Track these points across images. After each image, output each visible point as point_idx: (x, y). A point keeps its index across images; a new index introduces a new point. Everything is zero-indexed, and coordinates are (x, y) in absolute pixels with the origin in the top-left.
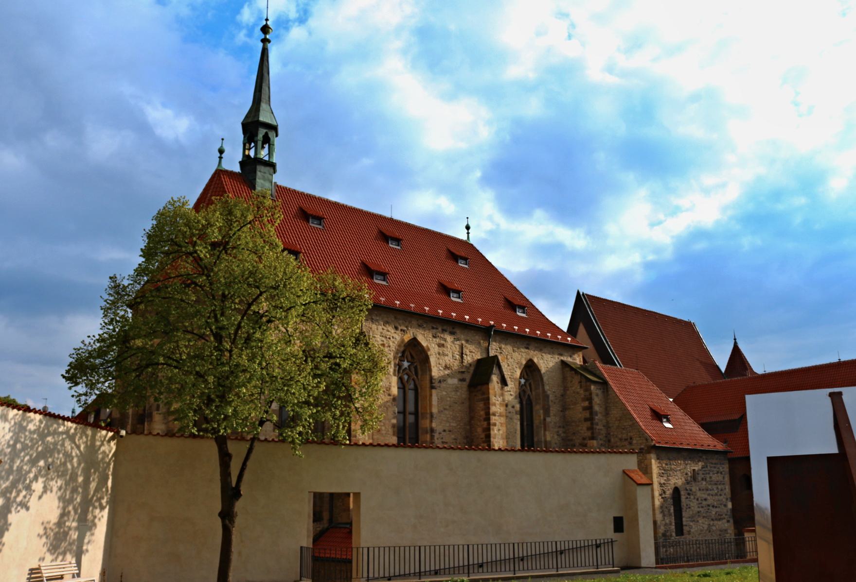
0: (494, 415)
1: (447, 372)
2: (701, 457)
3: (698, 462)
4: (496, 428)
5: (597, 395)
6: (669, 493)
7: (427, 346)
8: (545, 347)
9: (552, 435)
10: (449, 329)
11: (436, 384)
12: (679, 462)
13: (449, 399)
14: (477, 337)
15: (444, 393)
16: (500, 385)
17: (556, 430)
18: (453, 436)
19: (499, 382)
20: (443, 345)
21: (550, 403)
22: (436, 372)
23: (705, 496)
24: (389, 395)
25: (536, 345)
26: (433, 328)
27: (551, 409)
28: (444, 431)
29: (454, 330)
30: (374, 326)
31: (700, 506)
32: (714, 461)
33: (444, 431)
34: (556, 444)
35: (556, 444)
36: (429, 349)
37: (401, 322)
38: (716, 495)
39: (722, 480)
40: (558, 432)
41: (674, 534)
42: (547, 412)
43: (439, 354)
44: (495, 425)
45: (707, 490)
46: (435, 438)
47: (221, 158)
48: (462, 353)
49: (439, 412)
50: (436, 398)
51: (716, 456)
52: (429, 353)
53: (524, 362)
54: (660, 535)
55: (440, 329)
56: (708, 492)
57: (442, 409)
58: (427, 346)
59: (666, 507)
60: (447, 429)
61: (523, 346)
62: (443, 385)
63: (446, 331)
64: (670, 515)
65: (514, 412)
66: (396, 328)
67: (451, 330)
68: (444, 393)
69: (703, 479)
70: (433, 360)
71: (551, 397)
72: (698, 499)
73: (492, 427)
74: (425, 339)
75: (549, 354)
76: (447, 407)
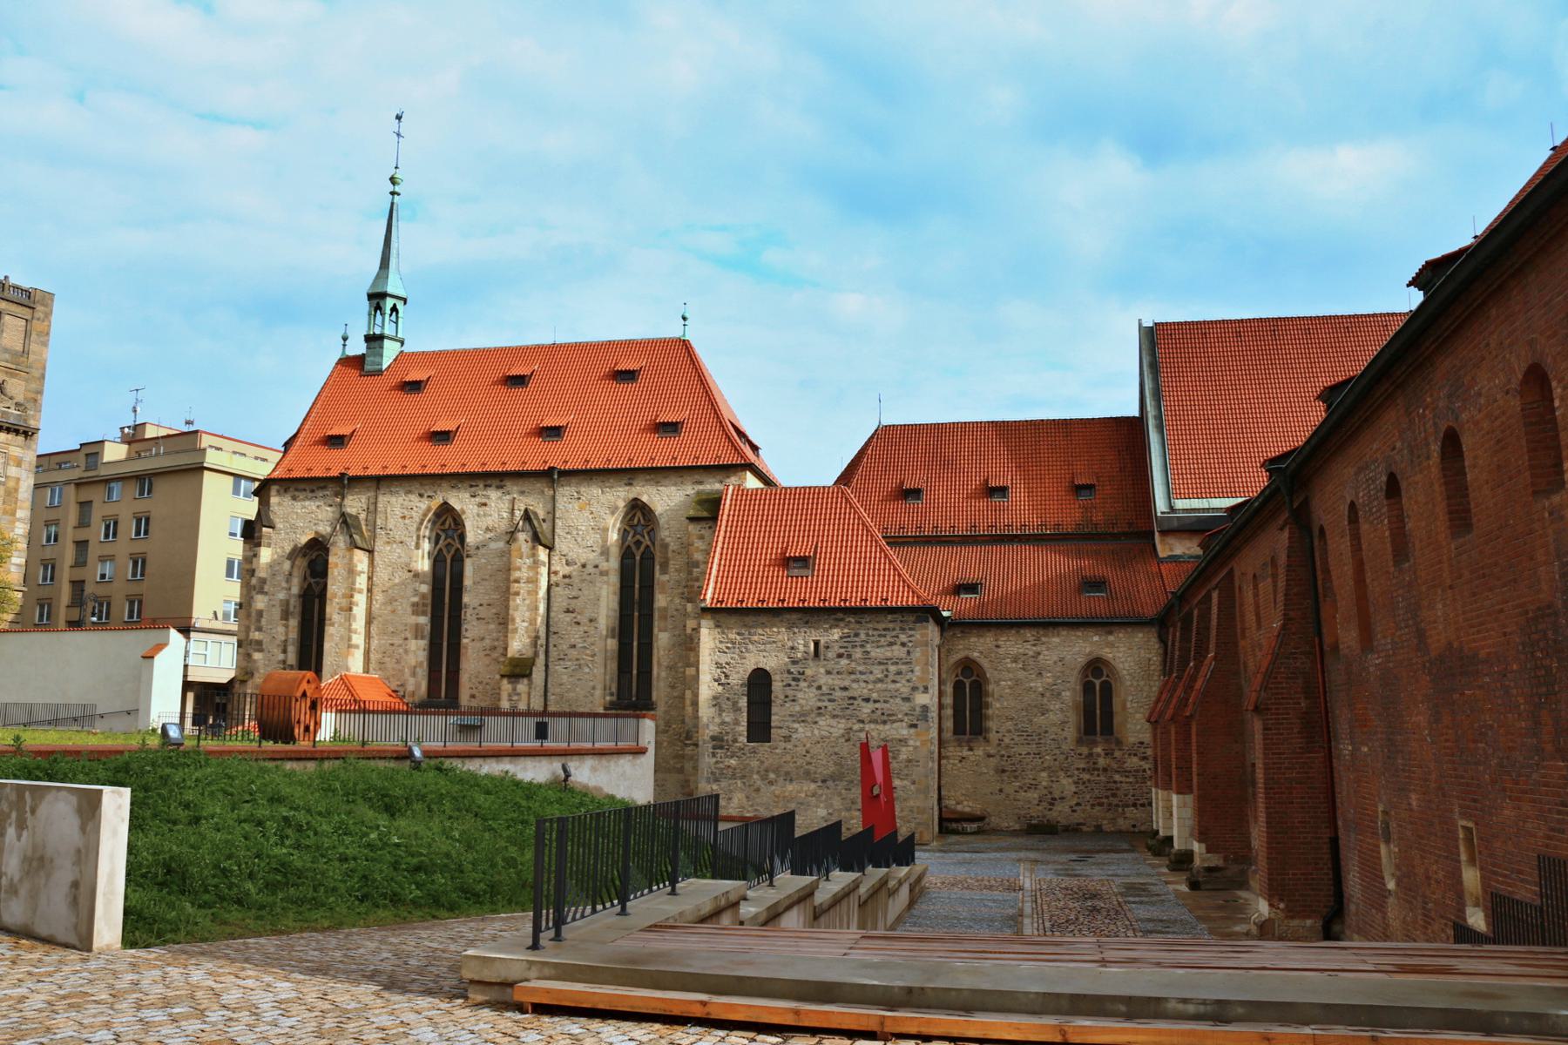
0: (517, 581)
2: (842, 620)
3: (831, 628)
4: (518, 600)
5: (701, 537)
6: (738, 677)
7: (462, 509)
8: (665, 478)
9: (669, 599)
10: (496, 482)
12: (775, 630)
13: (489, 567)
14: (539, 485)
15: (483, 561)
16: (530, 544)
17: (680, 591)
18: (494, 611)
19: (529, 540)
20: (485, 505)
21: (670, 555)
22: (471, 538)
23: (846, 683)
24: (410, 571)
25: (648, 477)
26: (471, 486)
27: (671, 562)
28: (481, 605)
29: (502, 483)
30: (393, 500)
31: (823, 698)
33: (481, 605)
34: (677, 610)
35: (677, 610)
36: (464, 512)
37: (427, 487)
38: (880, 681)
39: (904, 656)
40: (683, 594)
42: (664, 569)
43: (478, 515)
44: (517, 594)
45: (851, 673)
46: (468, 614)
47: (344, 345)
48: (513, 510)
49: (474, 583)
50: (471, 568)
51: (890, 617)
52: (463, 517)
53: (621, 504)
54: (707, 738)
55: (481, 486)
56: (853, 677)
57: (478, 580)
58: (462, 509)
59: (728, 699)
60: (484, 602)
61: (622, 483)
62: (482, 551)
63: (490, 486)
64: (737, 709)
65: (598, 573)
66: (421, 495)
67: (498, 483)
68: (483, 561)
69: (840, 656)
70: (468, 525)
71: (672, 546)
72: (819, 688)
73: (511, 597)
74: (461, 500)
75: (675, 485)
76: (487, 577)
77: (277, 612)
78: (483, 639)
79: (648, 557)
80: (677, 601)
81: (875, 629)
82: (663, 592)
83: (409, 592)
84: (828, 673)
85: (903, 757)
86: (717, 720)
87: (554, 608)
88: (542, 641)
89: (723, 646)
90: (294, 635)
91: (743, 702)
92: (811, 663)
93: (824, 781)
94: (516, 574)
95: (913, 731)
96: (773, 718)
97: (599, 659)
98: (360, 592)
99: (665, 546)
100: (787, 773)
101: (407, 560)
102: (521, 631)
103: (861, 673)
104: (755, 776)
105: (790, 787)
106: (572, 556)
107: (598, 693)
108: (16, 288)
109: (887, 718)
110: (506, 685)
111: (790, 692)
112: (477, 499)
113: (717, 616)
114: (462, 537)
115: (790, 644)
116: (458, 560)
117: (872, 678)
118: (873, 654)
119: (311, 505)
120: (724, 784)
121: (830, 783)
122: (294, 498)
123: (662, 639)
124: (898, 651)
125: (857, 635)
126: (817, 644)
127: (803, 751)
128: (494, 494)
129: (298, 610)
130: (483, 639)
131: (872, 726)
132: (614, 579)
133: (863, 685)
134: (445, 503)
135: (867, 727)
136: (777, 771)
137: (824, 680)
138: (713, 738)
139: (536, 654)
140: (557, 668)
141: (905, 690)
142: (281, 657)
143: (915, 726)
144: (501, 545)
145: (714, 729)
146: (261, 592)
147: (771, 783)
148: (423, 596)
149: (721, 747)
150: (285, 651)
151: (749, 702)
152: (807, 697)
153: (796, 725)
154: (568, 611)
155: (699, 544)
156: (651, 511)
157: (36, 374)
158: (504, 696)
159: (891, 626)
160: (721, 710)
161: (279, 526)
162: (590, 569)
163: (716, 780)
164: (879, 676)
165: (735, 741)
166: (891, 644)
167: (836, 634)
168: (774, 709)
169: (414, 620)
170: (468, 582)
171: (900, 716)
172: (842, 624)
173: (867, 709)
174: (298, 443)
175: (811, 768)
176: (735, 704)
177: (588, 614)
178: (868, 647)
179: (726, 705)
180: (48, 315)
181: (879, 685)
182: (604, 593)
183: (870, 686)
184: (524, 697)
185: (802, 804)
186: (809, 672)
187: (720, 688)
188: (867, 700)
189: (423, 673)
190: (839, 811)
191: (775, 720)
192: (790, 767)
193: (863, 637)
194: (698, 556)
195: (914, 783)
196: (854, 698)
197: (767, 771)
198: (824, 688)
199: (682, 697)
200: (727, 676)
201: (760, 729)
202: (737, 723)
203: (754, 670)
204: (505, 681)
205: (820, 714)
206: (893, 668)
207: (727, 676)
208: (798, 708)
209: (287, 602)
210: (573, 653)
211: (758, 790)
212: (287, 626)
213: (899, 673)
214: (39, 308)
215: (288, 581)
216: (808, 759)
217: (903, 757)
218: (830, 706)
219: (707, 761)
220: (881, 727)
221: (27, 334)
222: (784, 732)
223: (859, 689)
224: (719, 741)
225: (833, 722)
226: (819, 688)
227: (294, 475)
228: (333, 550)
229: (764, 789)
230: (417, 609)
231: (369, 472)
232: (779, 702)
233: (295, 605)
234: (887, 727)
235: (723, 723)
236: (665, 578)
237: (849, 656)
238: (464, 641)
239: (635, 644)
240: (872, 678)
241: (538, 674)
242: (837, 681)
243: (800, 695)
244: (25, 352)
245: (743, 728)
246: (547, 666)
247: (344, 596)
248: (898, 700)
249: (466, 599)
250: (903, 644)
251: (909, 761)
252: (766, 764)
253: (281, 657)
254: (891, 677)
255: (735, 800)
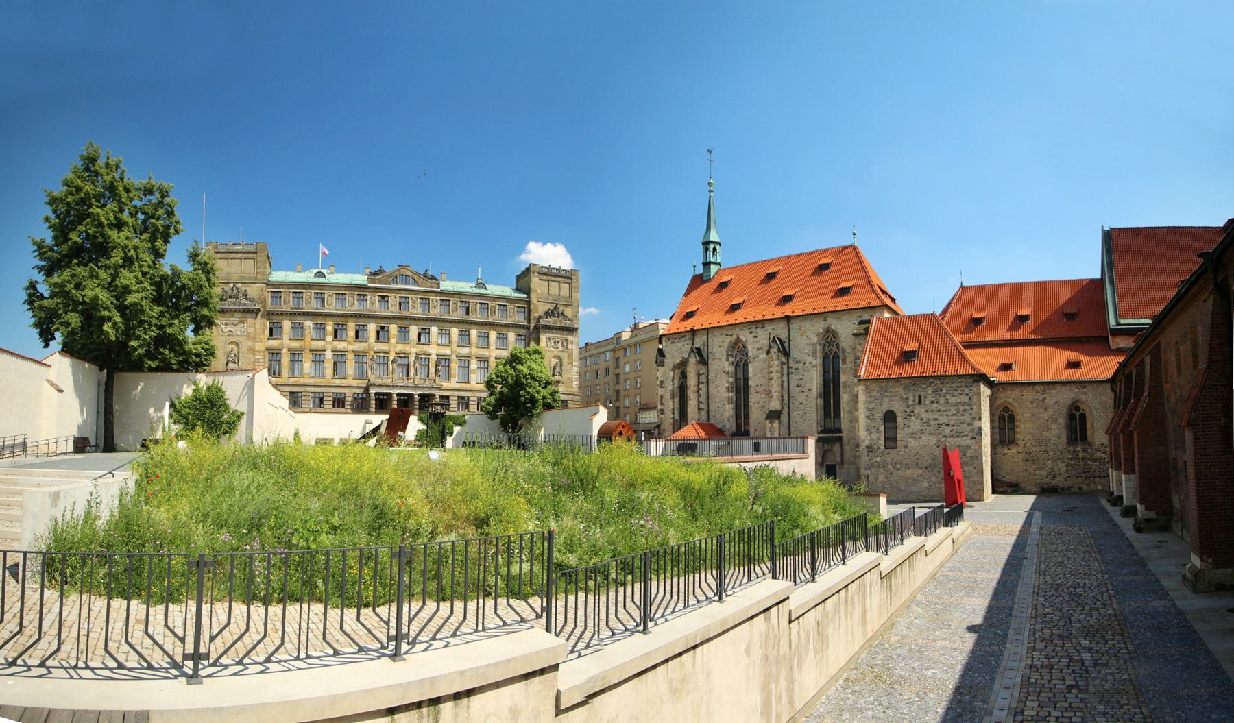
0: (771, 373)
1: (760, 351)
2: (933, 382)
4: (773, 382)
5: (860, 344)
10: (760, 325)
11: (752, 360)
21: (847, 354)
23: (936, 417)
32: (954, 385)
36: (746, 341)
41: (883, 447)
42: (844, 363)
44: (772, 379)
45: (940, 411)
51: (959, 380)
53: (821, 331)
62: (756, 360)
66: (727, 335)
69: (932, 402)
70: (749, 347)
71: (848, 350)
72: (922, 419)
77: (668, 397)
78: (759, 402)
79: (836, 356)
80: (852, 377)
81: (951, 387)
82: (843, 374)
83: (725, 381)
84: (927, 411)
85: (968, 455)
86: (869, 438)
87: (791, 385)
88: (786, 401)
89: (870, 399)
90: (677, 406)
91: (882, 428)
92: (917, 406)
93: (926, 468)
94: (772, 369)
95: (973, 441)
96: (898, 436)
97: (814, 409)
98: (702, 383)
99: (844, 350)
100: (907, 464)
101: (722, 367)
102: (775, 397)
103: (944, 411)
104: (890, 466)
105: (908, 472)
106: (798, 358)
107: (815, 425)
108: (564, 270)
109: (958, 435)
110: (768, 424)
111: (906, 423)
112: (753, 335)
113: (867, 383)
114: (747, 354)
115: (905, 396)
116: (746, 365)
117: (950, 413)
118: (950, 401)
119: (680, 345)
120: (874, 470)
121: (929, 469)
122: (673, 343)
123: (845, 398)
124: (964, 399)
125: (941, 390)
126: (920, 396)
127: (913, 452)
128: (760, 332)
129: (678, 393)
130: (759, 402)
131: (951, 439)
132: (820, 369)
133: (945, 417)
134: (738, 338)
135: (948, 440)
136: (901, 463)
137: (925, 416)
138: (867, 447)
139: (783, 408)
140: (794, 414)
141: (969, 420)
142: (672, 416)
143: (975, 438)
144: (765, 355)
145: (867, 443)
146: (661, 387)
147: (898, 470)
148: (732, 383)
149: (872, 452)
150: (673, 413)
151: (885, 428)
152: (915, 425)
153: (910, 440)
154: (798, 386)
155: (859, 347)
156: (836, 333)
157: (575, 305)
158: (768, 430)
159: (960, 385)
160: (871, 433)
161: (667, 356)
162: (807, 364)
163: (870, 469)
164: (955, 412)
165: (879, 448)
166: (961, 394)
167: (930, 391)
168: (898, 432)
169: (727, 395)
170: (750, 375)
171: (966, 433)
172: (933, 385)
173: (948, 430)
174: (674, 318)
175: (920, 462)
176: (878, 429)
177: (808, 386)
178: (948, 397)
179: (874, 430)
180: (577, 280)
181: (954, 417)
182: (815, 376)
183: (949, 418)
184: (777, 430)
185: (914, 480)
186: (916, 412)
187: (869, 422)
188: (948, 425)
189: (733, 420)
190: (935, 483)
191: (899, 437)
192: (908, 461)
193: (944, 391)
194: (859, 354)
195: (975, 468)
196: (941, 424)
197: (896, 463)
198: (924, 420)
199: (854, 427)
200: (873, 415)
201: (891, 441)
202: (879, 439)
203: (886, 412)
204: (768, 422)
205: (922, 433)
206: (962, 408)
207: (873, 415)
208: (911, 431)
209: (673, 390)
210: (802, 407)
211: (891, 473)
212: (673, 402)
213: (965, 410)
214: (573, 277)
215: (673, 381)
216: (917, 457)
217: (968, 455)
218: (928, 428)
219: (864, 460)
220: (956, 439)
221: (570, 289)
222: (904, 443)
223: (943, 420)
224: (870, 449)
225: (930, 437)
226: (922, 419)
227: (672, 332)
228: (689, 364)
229: (894, 472)
230: (729, 390)
231: (703, 327)
232: (900, 427)
233: (676, 391)
234: (959, 439)
235: (872, 439)
236: (845, 366)
237: (938, 402)
238: (750, 404)
239: (832, 401)
240: (950, 413)
241: (784, 418)
242: (931, 416)
243: (912, 424)
244: (570, 296)
245: (882, 441)
246: (789, 414)
247: (695, 386)
248: (965, 425)
249: (750, 383)
250: (967, 394)
251: (972, 457)
252: (895, 460)
253: (672, 416)
254: (961, 413)
255: (880, 479)
